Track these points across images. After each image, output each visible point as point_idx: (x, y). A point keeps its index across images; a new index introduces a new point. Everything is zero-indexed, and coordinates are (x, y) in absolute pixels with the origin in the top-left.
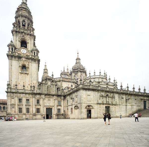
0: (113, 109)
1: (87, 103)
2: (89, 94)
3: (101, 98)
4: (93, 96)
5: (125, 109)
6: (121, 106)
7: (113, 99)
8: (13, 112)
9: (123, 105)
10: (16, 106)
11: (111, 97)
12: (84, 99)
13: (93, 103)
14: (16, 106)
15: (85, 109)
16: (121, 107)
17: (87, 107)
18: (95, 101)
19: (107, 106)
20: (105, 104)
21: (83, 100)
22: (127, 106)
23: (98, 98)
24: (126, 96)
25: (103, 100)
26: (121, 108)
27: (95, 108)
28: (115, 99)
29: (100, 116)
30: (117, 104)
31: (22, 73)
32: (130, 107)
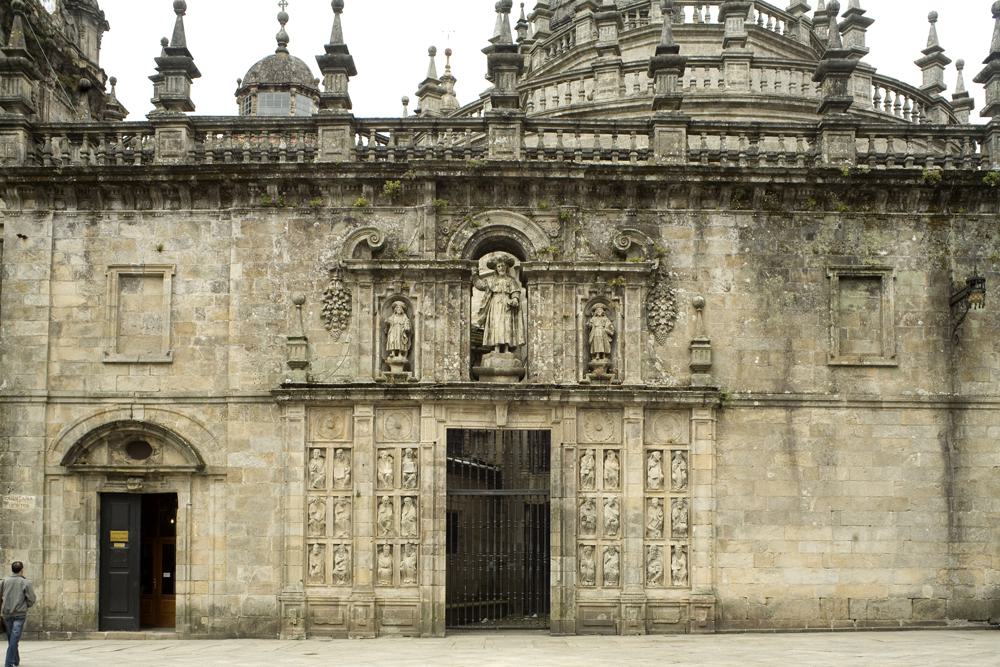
0: (618, 481)
1: (96, 398)
2: (145, 257)
3: (363, 298)
4: (203, 287)
5: (937, 475)
7: (632, 303)
9: (875, 405)
11: (576, 278)
12: (55, 329)
13: (209, 387)
15: (72, 485)
16: (828, 439)
17: (102, 457)
18: (237, 355)
19: (472, 422)
20: (438, 394)
21: (27, 357)
22: (972, 419)
23: (313, 311)
24: (954, 240)
25: (395, 338)
26: (830, 462)
27: (235, 460)
28: (683, 293)
29: (329, 592)
30: (728, 377)
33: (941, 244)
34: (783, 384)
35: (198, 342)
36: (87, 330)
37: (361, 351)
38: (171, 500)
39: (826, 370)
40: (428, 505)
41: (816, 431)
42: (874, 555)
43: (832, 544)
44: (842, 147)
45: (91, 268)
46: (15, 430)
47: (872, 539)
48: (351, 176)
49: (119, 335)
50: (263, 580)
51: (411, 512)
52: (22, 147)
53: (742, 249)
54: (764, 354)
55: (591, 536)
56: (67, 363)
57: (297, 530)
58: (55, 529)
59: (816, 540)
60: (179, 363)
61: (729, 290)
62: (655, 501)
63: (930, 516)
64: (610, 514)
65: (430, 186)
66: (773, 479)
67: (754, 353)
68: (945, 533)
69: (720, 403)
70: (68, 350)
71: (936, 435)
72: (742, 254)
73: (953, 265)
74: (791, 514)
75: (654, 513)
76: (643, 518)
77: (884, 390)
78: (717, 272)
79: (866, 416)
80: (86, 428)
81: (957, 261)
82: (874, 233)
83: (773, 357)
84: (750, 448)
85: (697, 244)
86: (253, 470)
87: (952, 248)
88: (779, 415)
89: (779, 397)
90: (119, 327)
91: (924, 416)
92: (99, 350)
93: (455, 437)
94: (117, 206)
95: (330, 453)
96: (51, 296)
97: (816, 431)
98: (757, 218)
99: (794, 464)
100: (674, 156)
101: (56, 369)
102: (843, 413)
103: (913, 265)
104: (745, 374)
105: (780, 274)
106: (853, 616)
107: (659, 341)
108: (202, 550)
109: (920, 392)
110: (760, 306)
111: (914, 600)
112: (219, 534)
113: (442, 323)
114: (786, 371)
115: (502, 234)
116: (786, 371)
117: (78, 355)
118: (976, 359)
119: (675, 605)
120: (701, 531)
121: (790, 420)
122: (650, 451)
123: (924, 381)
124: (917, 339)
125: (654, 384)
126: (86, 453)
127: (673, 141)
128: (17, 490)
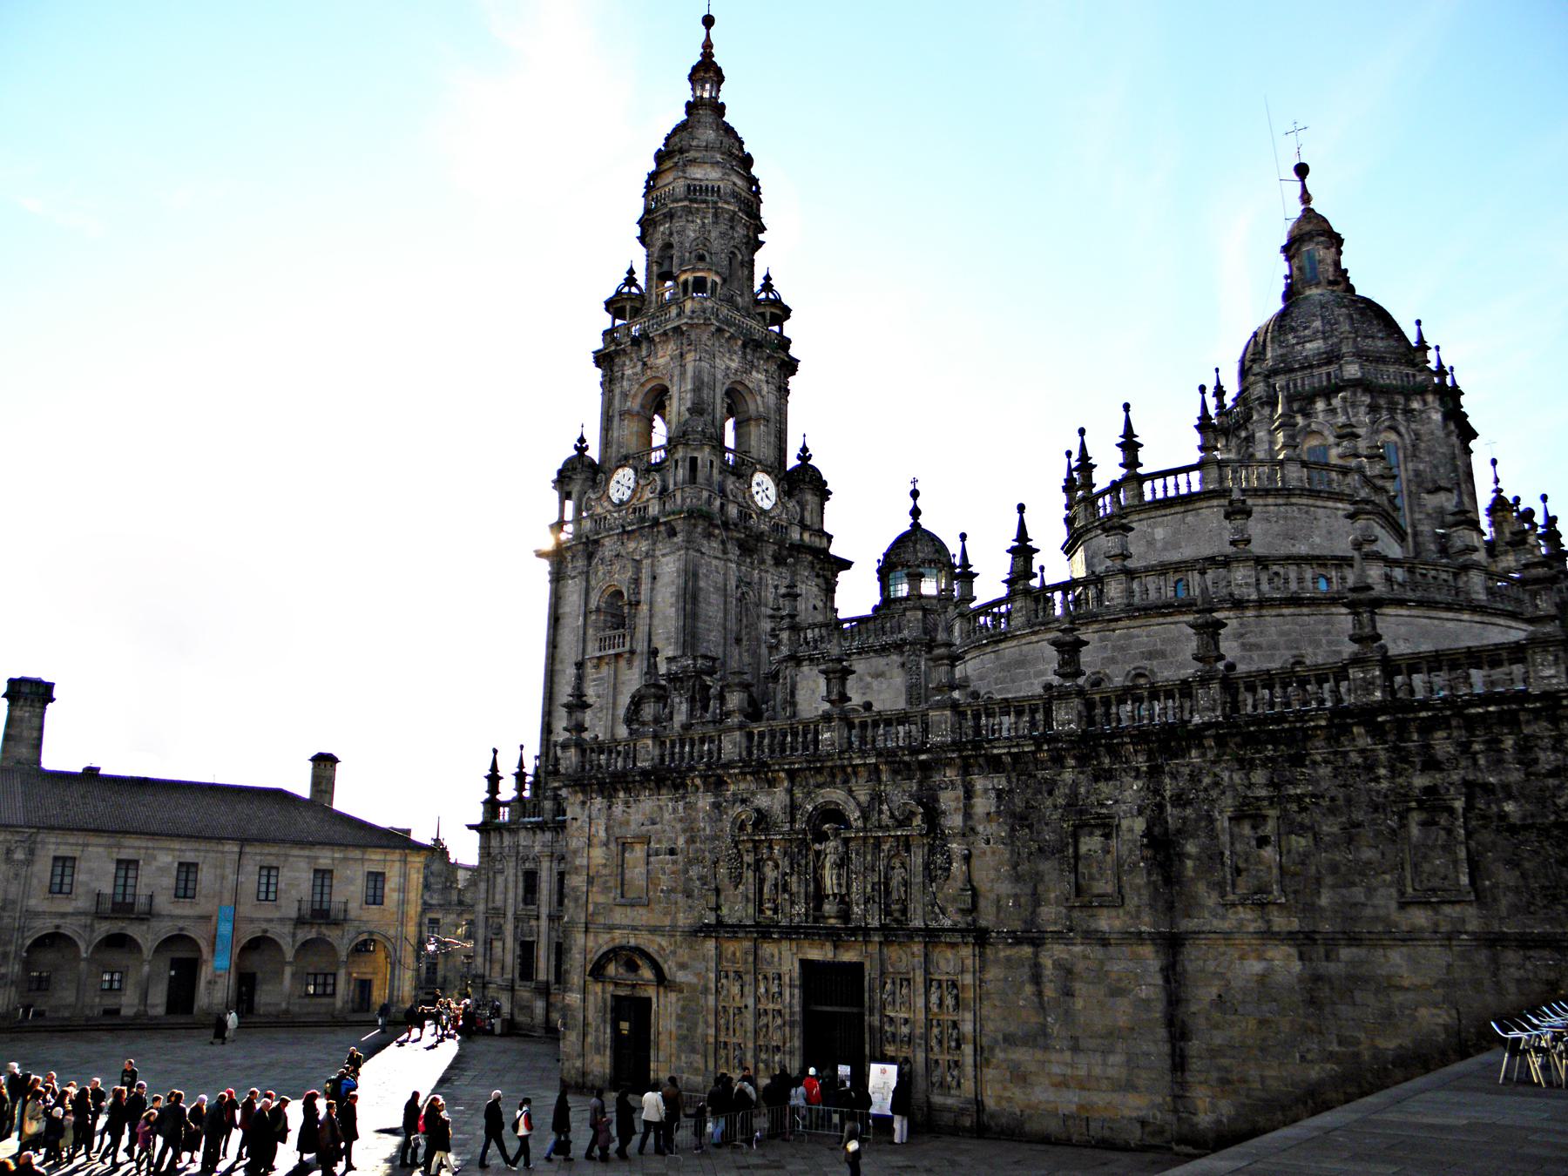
1: (611, 928)
6: (1053, 953)
8: (497, 968)
9: (1104, 942)
10: (509, 928)
12: (590, 881)
13: (667, 921)
14: (509, 928)
19: (815, 954)
21: (576, 900)
26: (1069, 993)
27: (681, 977)
28: (955, 846)
30: (987, 919)
31: (600, 658)
32: (1284, 963)
33: (1157, 792)
34: (1031, 921)
35: (662, 891)
36: (606, 882)
37: (748, 899)
38: (649, 999)
39: (1064, 911)
40: (787, 1017)
41: (1058, 965)
42: (1108, 1078)
43: (1072, 1067)
44: (1067, 714)
45: (608, 839)
46: (571, 949)
47: (1105, 1064)
48: (737, 771)
49: (622, 884)
50: (695, 1065)
51: (779, 1021)
52: (573, 759)
53: (998, 807)
54: (1016, 897)
55: (893, 1048)
56: (596, 905)
57: (712, 1031)
58: (590, 1019)
59: (1059, 1062)
60: (652, 905)
61: (988, 842)
62: (935, 1022)
63: (1156, 1046)
64: (905, 1030)
65: (782, 775)
66: (1023, 1007)
67: (1009, 896)
68: (1169, 1062)
69: (981, 937)
70: (597, 897)
71: (1157, 969)
72: (998, 813)
73: (1169, 808)
74: (1037, 1038)
75: (936, 1031)
76: (926, 1037)
77: (1111, 927)
78: (980, 828)
79: (1097, 952)
80: (605, 949)
81: (1173, 806)
82: (1102, 785)
83: (1023, 900)
84: (1006, 979)
85: (965, 805)
86: (689, 985)
87: (1168, 794)
88: (1027, 950)
89: (1026, 935)
90: (623, 880)
91: (1147, 950)
92: (612, 895)
93: (806, 964)
94: (621, 794)
95: (732, 975)
96: (589, 857)
97: (1058, 965)
98: (1009, 781)
99: (1040, 994)
100: (942, 736)
101: (591, 908)
102: (1077, 949)
103: (1135, 812)
104: (1002, 915)
105: (1027, 827)
106: (1092, 1133)
107: (940, 888)
108: (664, 1038)
109: (1144, 928)
110: (1012, 855)
111: (1143, 1123)
112: (674, 1029)
113: (794, 878)
114: (1033, 912)
115: (833, 806)
116: (1033, 912)
117: (601, 899)
118: (1192, 897)
119: (949, 1109)
120: (968, 1049)
121: (1036, 955)
122: (932, 980)
123: (1147, 919)
124: (1141, 880)
125: (933, 925)
126: (604, 968)
127: (940, 722)
128: (571, 990)
